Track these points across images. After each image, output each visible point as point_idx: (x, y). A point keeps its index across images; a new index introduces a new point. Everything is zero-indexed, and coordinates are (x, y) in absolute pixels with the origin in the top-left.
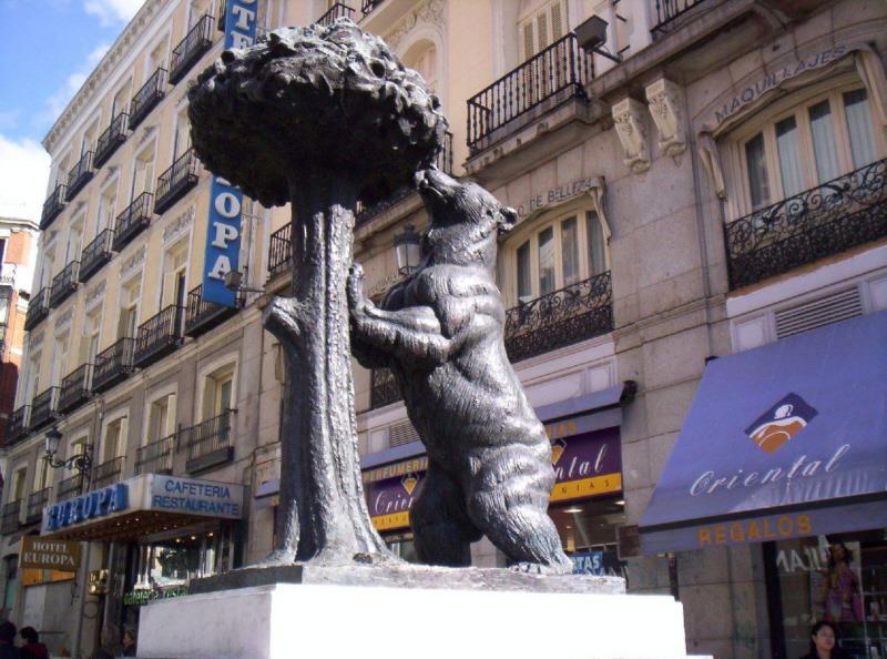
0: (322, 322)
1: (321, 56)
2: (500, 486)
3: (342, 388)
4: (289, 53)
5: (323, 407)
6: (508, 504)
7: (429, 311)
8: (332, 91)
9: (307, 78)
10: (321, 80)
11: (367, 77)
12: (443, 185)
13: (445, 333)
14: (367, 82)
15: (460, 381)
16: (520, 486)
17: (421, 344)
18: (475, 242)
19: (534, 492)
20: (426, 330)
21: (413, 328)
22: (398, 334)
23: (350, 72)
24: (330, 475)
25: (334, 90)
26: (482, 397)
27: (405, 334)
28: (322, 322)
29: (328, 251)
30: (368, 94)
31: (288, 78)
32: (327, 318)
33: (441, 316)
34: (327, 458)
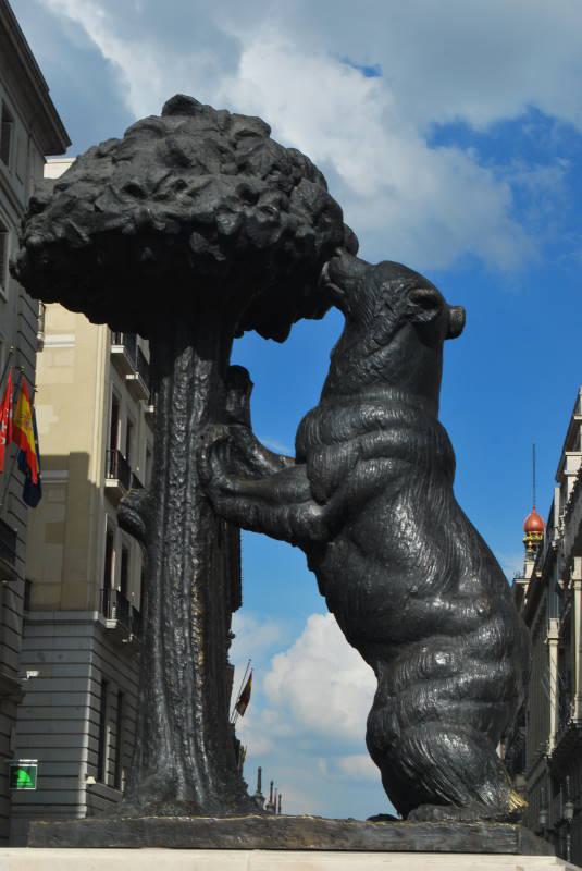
0: (161, 513)
1: (67, 200)
2: (394, 698)
3: (182, 596)
8: (87, 239)
9: (54, 234)
10: (69, 229)
11: (115, 208)
12: (345, 277)
14: (113, 216)
15: (354, 558)
17: (280, 518)
18: (365, 356)
19: (444, 706)
23: (97, 209)
24: (160, 708)
25: (89, 236)
30: (118, 230)
32: (167, 509)
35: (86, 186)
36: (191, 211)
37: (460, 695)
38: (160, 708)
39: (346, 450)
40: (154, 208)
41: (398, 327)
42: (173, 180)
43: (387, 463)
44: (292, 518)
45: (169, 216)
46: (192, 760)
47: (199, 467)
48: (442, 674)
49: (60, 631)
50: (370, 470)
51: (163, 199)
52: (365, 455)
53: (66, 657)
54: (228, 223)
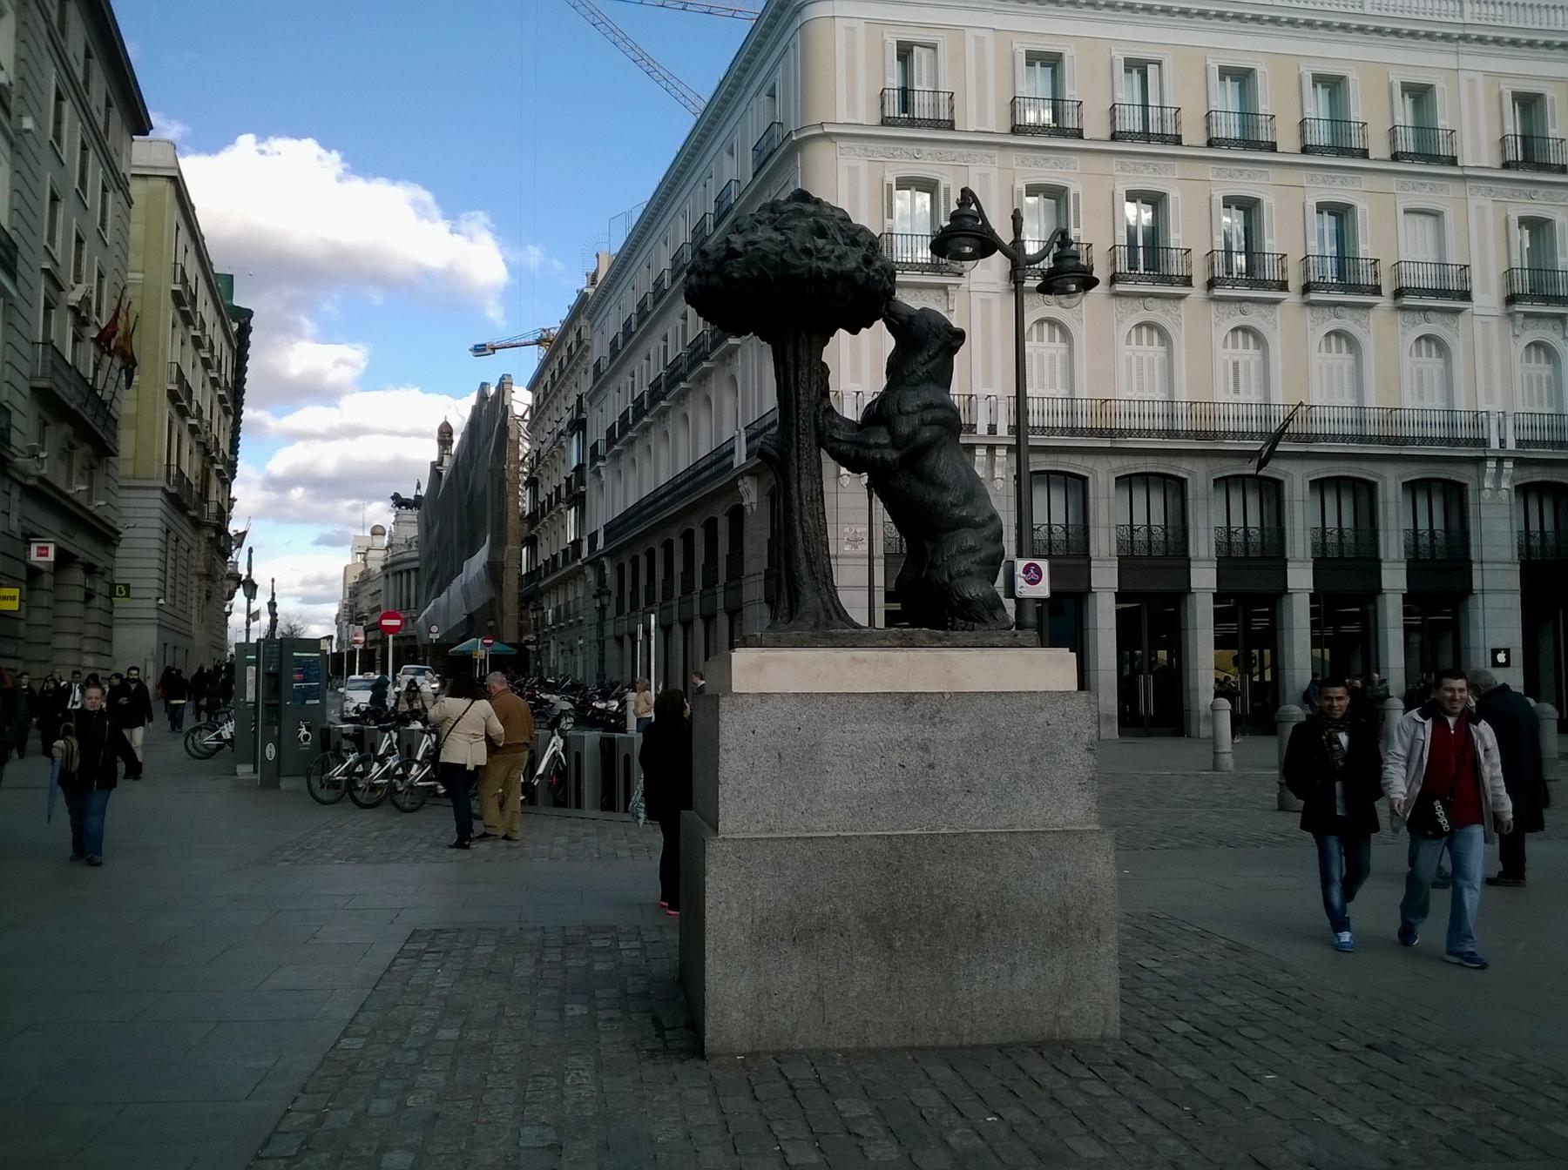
0: (794, 450)
4: (738, 254)
5: (797, 517)
6: (950, 576)
7: (883, 430)
13: (895, 445)
14: (796, 267)
16: (964, 563)
19: (974, 568)
20: (878, 446)
21: (869, 447)
22: (857, 453)
23: (783, 261)
26: (931, 495)
27: (862, 452)
28: (794, 450)
29: (798, 393)
31: (736, 275)
33: (892, 433)
34: (801, 555)
35: (770, 245)
36: (839, 269)
37: (982, 562)
38: (803, 567)
39: (916, 420)
40: (815, 263)
41: (941, 349)
42: (829, 247)
43: (936, 428)
44: (882, 458)
45: (830, 271)
46: (826, 597)
47: (816, 421)
48: (972, 550)
49: (134, 493)
50: (926, 434)
51: (826, 259)
52: (924, 424)
53: (140, 513)
54: (860, 278)
